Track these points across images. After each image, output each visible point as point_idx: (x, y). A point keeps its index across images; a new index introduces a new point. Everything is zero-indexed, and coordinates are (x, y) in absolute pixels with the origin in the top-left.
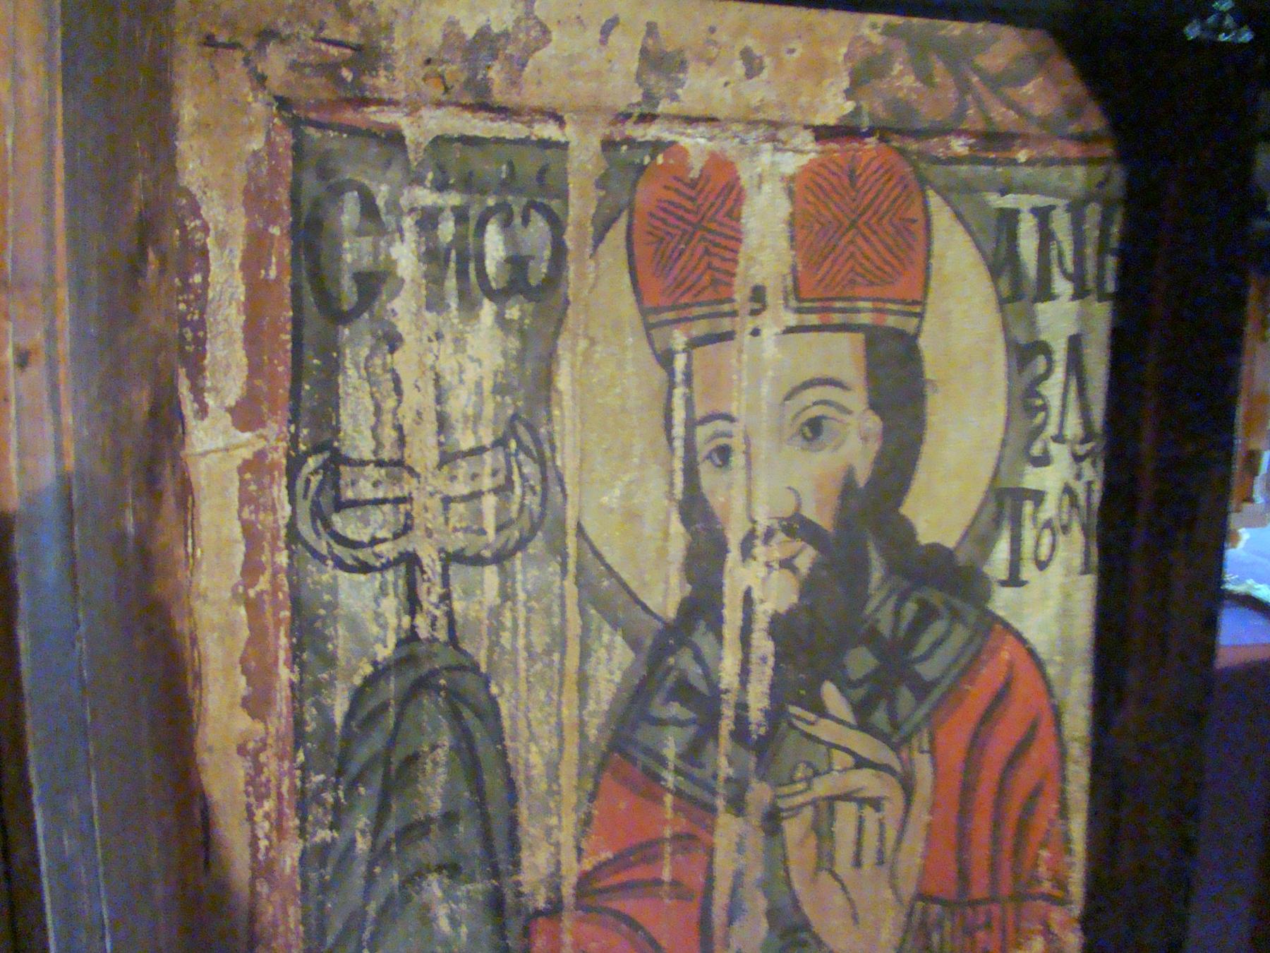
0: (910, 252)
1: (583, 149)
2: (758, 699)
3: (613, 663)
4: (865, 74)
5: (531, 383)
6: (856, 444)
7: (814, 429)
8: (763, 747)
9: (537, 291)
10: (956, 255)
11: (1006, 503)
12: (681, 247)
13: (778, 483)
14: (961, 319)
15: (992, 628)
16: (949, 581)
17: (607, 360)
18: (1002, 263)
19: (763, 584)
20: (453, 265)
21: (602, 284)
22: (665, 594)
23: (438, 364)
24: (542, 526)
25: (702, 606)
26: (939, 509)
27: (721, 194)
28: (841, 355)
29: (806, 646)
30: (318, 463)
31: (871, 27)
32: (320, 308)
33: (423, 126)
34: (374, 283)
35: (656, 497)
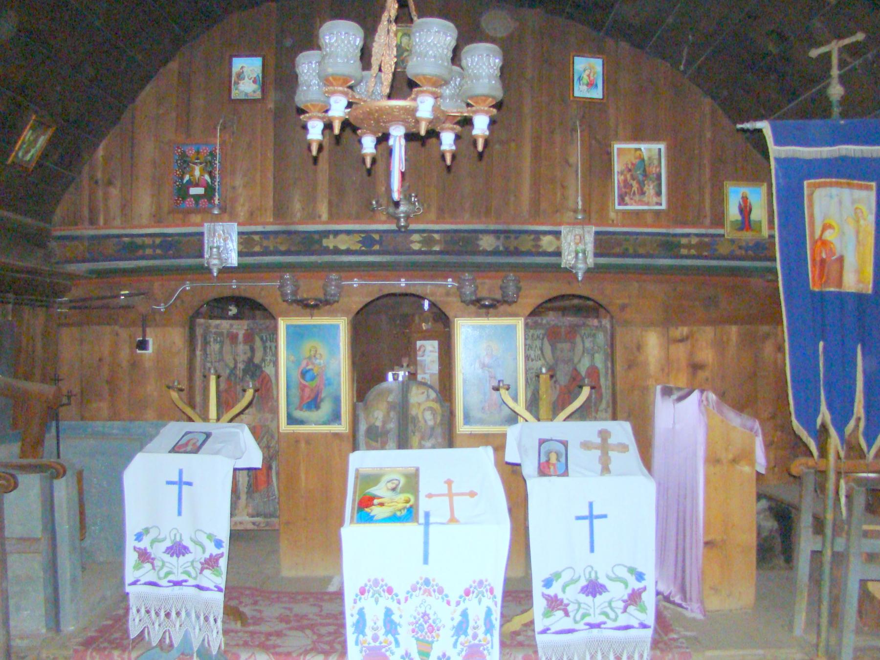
2: (241, 375)
3: (228, 371)
4: (248, 325)
5: (222, 347)
6: (249, 354)
7: (245, 353)
8: (242, 380)
9: (222, 343)
10: (257, 339)
11: (263, 360)
13: (242, 357)
14: (258, 343)
15: (262, 372)
16: (258, 367)
17: (227, 348)
18: (262, 339)
19: (241, 366)
20: (215, 341)
21: (227, 342)
22: (232, 366)
23: (215, 347)
24: (221, 360)
25: (235, 367)
26: (257, 361)
27: (237, 335)
28: (247, 347)
29: (245, 371)
30: (205, 354)
32: (206, 343)
33: (214, 331)
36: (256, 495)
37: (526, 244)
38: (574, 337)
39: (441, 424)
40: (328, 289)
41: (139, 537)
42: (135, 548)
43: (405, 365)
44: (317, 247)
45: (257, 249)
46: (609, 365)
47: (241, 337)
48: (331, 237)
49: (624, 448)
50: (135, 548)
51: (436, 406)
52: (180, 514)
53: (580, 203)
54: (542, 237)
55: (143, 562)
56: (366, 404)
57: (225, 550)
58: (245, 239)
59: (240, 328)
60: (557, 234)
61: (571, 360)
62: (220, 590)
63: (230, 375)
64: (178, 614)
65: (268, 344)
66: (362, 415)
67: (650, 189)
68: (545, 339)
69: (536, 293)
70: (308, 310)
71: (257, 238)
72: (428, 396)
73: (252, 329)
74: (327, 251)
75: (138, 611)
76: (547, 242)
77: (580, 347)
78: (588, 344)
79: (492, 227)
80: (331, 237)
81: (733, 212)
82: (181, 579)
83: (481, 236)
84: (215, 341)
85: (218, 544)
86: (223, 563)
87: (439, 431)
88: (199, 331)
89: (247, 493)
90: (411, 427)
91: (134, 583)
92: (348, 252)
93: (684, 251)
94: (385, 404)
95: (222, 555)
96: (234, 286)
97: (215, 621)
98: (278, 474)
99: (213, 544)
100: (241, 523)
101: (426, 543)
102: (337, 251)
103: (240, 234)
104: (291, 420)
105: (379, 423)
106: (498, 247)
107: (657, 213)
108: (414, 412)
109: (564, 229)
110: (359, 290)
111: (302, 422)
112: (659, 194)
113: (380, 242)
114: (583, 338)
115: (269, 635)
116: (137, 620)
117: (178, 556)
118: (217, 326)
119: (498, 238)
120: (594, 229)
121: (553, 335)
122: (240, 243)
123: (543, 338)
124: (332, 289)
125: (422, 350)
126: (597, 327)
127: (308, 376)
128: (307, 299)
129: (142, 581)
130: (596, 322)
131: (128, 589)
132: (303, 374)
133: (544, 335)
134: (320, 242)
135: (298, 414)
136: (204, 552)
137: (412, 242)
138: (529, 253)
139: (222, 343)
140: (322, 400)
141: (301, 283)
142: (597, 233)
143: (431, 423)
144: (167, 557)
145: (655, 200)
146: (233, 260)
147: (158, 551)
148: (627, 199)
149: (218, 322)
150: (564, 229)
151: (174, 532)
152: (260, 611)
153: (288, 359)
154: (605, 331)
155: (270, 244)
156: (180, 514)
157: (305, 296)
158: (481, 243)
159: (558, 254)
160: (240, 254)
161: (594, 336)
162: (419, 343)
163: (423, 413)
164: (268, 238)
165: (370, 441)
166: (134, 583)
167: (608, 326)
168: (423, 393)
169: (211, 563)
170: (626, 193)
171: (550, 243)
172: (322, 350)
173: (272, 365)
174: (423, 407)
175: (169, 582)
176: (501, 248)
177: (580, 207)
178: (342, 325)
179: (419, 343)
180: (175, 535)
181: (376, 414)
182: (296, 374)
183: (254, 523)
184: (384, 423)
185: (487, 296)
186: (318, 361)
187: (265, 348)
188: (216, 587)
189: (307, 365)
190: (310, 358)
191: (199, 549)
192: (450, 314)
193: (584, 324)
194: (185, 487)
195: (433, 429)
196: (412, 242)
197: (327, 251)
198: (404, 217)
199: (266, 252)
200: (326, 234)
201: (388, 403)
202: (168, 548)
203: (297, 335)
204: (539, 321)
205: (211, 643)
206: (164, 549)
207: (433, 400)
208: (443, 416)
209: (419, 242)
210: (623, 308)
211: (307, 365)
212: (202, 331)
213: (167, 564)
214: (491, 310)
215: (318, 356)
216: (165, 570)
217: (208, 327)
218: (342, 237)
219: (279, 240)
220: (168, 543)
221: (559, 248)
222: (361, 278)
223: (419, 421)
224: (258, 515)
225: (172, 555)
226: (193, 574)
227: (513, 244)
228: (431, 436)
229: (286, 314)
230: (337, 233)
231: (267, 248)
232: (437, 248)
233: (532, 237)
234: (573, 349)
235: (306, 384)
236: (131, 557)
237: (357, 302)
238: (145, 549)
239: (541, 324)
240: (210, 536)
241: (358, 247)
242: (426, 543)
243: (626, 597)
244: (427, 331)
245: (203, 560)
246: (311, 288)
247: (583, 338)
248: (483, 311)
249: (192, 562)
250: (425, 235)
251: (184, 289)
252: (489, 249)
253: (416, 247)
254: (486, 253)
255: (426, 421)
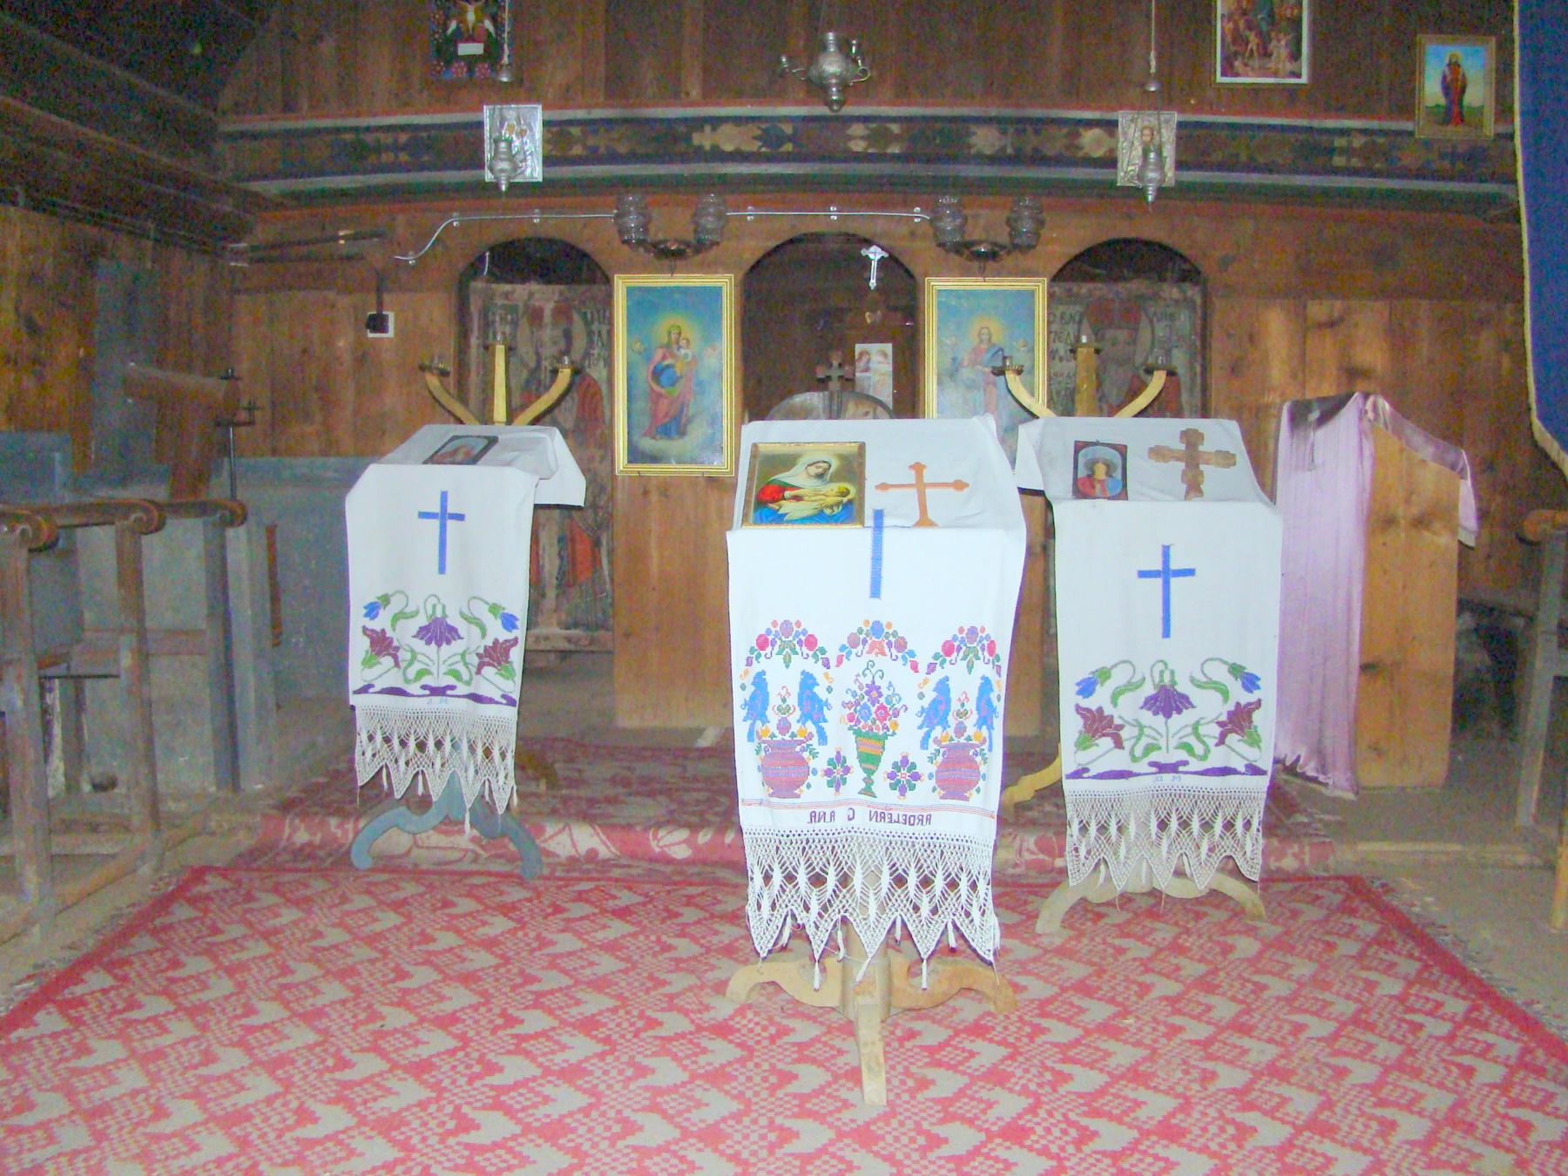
0: (570, 320)
1: (521, 305)
3: (525, 375)
4: (561, 294)
7: (555, 343)
9: (515, 323)
10: (576, 317)
12: (536, 316)
14: (578, 327)
20: (503, 319)
21: (524, 322)
22: (533, 365)
31: (562, 287)
32: (487, 325)
34: (494, 322)
35: (531, 350)
36: (574, 592)
37: (1055, 143)
38: (1137, 321)
40: (702, 221)
41: (372, 610)
42: (365, 630)
43: (835, 363)
44: (682, 147)
45: (577, 150)
46: (1198, 369)
47: (547, 314)
48: (708, 129)
49: (1227, 459)
50: (365, 630)
52: (442, 570)
53: (1153, 63)
54: (1081, 130)
55: (379, 654)
57: (520, 633)
58: (556, 132)
59: (544, 295)
60: (1110, 126)
61: (1129, 360)
62: (511, 702)
63: (528, 382)
64: (439, 744)
65: (595, 327)
67: (1280, 48)
68: (1085, 321)
69: (1070, 234)
70: (666, 262)
71: (575, 131)
73: (566, 300)
74: (699, 155)
75: (371, 738)
76: (1091, 141)
77: (1145, 334)
78: (1161, 331)
79: (993, 112)
80: (708, 129)
81: (1432, 90)
82: (443, 684)
83: (973, 128)
84: (503, 319)
85: (509, 622)
86: (516, 656)
88: (474, 308)
89: (558, 586)
91: (364, 690)
92: (739, 156)
93: (1339, 161)
95: (516, 641)
96: (538, 221)
97: (503, 756)
98: (611, 552)
99: (499, 622)
100: (547, 638)
101: (877, 559)
102: (718, 155)
103: (546, 124)
104: (635, 455)
106: (1003, 149)
107: (1292, 93)
109: (1122, 117)
110: (757, 226)
111: (654, 459)
112: (1295, 56)
113: (791, 139)
114: (1151, 322)
115: (592, 802)
116: (369, 754)
117: (439, 645)
118: (506, 295)
119: (1004, 133)
120: (1176, 117)
121: (1100, 317)
122: (546, 141)
123: (1080, 322)
124: (709, 222)
125: (865, 359)
126: (1177, 302)
127: (664, 379)
128: (666, 241)
129: (378, 688)
130: (1175, 293)
131: (354, 700)
132: (657, 374)
133: (1082, 315)
134: (688, 139)
135: (647, 444)
136: (484, 635)
137: (850, 138)
138: (1058, 161)
139: (515, 323)
140: (689, 421)
141: (655, 213)
142: (1180, 125)
144: (419, 645)
145: (1289, 66)
146: (534, 171)
147: (405, 635)
148: (1237, 63)
149: (508, 287)
150: (1122, 117)
151: (433, 600)
152: (579, 771)
153: (630, 348)
154: (1194, 308)
155: (600, 141)
156: (442, 570)
157: (661, 236)
158: (973, 140)
159: (1111, 162)
160: (548, 161)
161: (1172, 317)
162: (859, 348)
164: (596, 132)
166: (364, 690)
167: (1198, 300)
169: (495, 655)
170: (1236, 54)
171: (1099, 143)
172: (691, 330)
173: (602, 364)
175: (424, 687)
176: (1009, 151)
177: (1153, 70)
178: (725, 284)
179: (859, 348)
180: (434, 606)
182: (644, 374)
183: (569, 640)
185: (983, 237)
186: (683, 351)
187: (590, 334)
188: (503, 696)
189: (664, 358)
190: (668, 346)
191: (476, 631)
192: (916, 270)
193: (1155, 296)
194: (451, 524)
196: (850, 138)
197: (699, 155)
198: (836, 85)
199: (594, 157)
200: (698, 123)
202: (421, 629)
203: (644, 304)
204: (1075, 289)
205: (495, 795)
206: (415, 630)
209: (862, 138)
210: (1225, 263)
211: (664, 358)
212: (480, 303)
213: (420, 657)
214: (991, 264)
215: (683, 343)
216: (417, 667)
217: (490, 297)
218: (727, 129)
219: (615, 135)
220: (422, 621)
221: (1112, 151)
222: (756, 205)
224: (576, 625)
225: (428, 643)
226: (466, 676)
227: (1031, 141)
229: (628, 268)
230: (716, 122)
231: (595, 150)
232: (895, 149)
233: (1065, 130)
234: (1134, 341)
235: (663, 391)
236: (358, 645)
237: (753, 249)
238: (383, 631)
239: (1078, 295)
240: (494, 609)
241: (754, 146)
242: (877, 559)
243: (1224, 718)
244: (872, 327)
245: (481, 651)
246: (671, 223)
247: (1151, 322)
248: (976, 264)
249: (463, 655)
250: (874, 125)
251: (449, 227)
252: (988, 152)
253: (858, 146)
254: (982, 159)
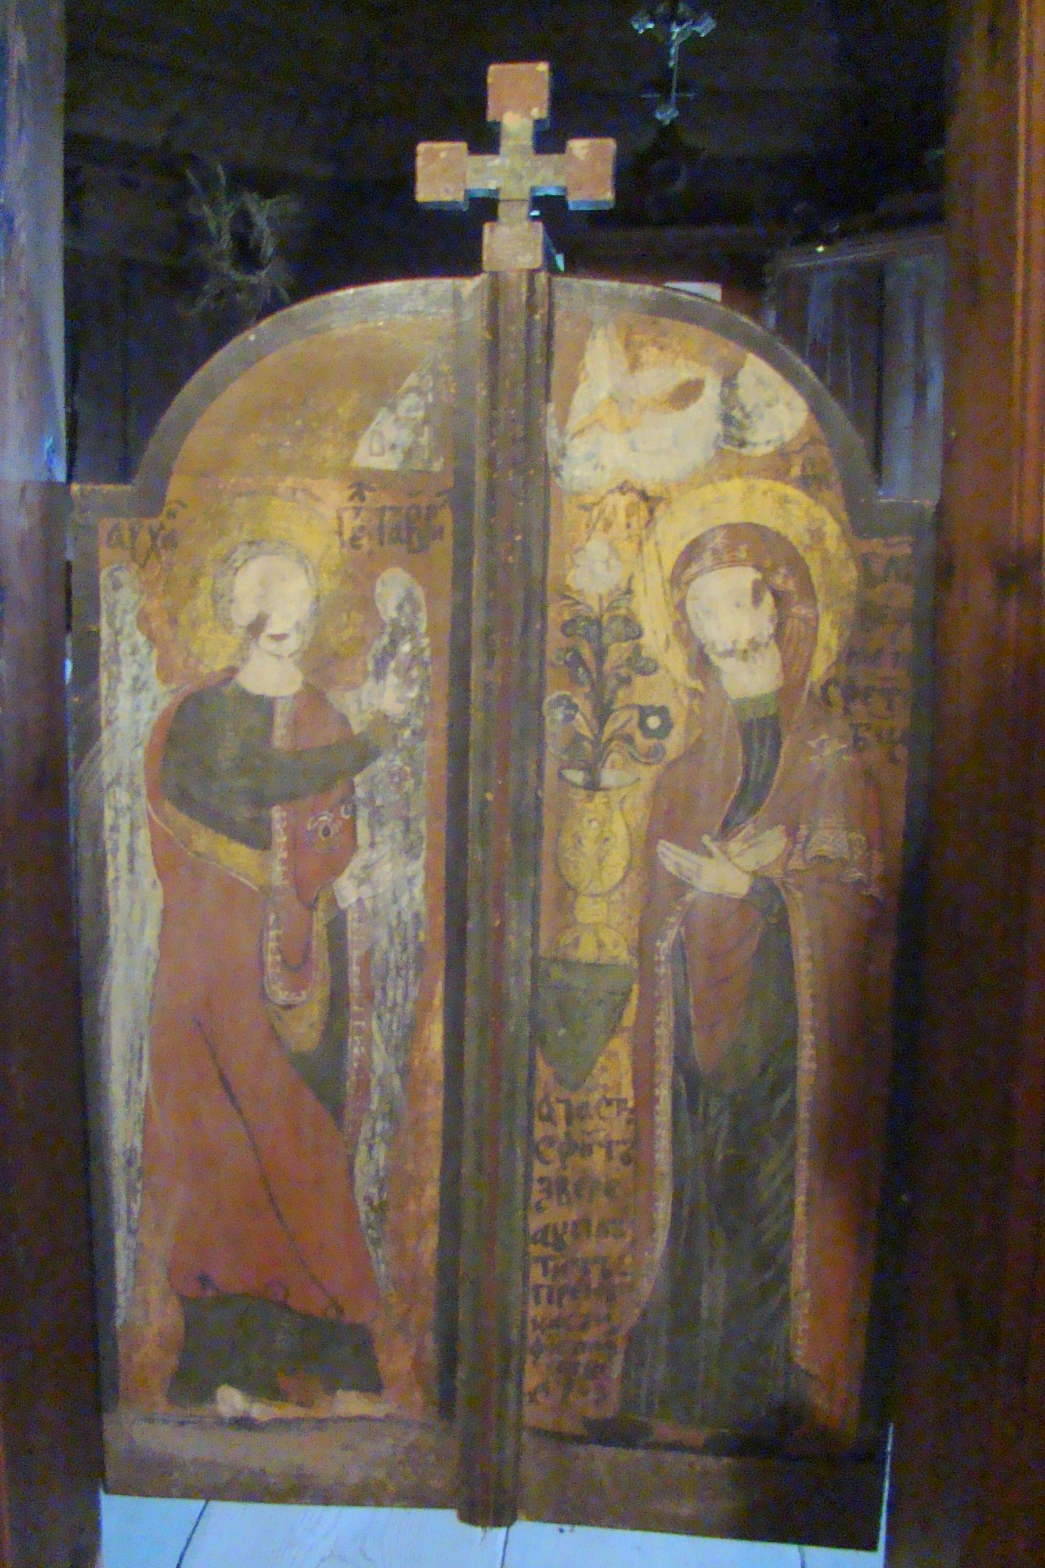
39: (848, 689)
51: (801, 515)
56: (153, 501)
66: (122, 606)
72: (733, 424)
87: (824, 753)
90: (564, 714)
94: (334, 496)
105: (272, 675)
108: (590, 569)
143: (752, 680)
163: (678, 579)
165: (204, 840)
168: (686, 394)
174: (675, 530)
181: (247, 588)
184: (322, 664)
195: (763, 731)
201: (361, 485)
207: (778, 465)
208: (866, 615)
223: (642, 665)
228: (749, 798)
255: (701, 663)
